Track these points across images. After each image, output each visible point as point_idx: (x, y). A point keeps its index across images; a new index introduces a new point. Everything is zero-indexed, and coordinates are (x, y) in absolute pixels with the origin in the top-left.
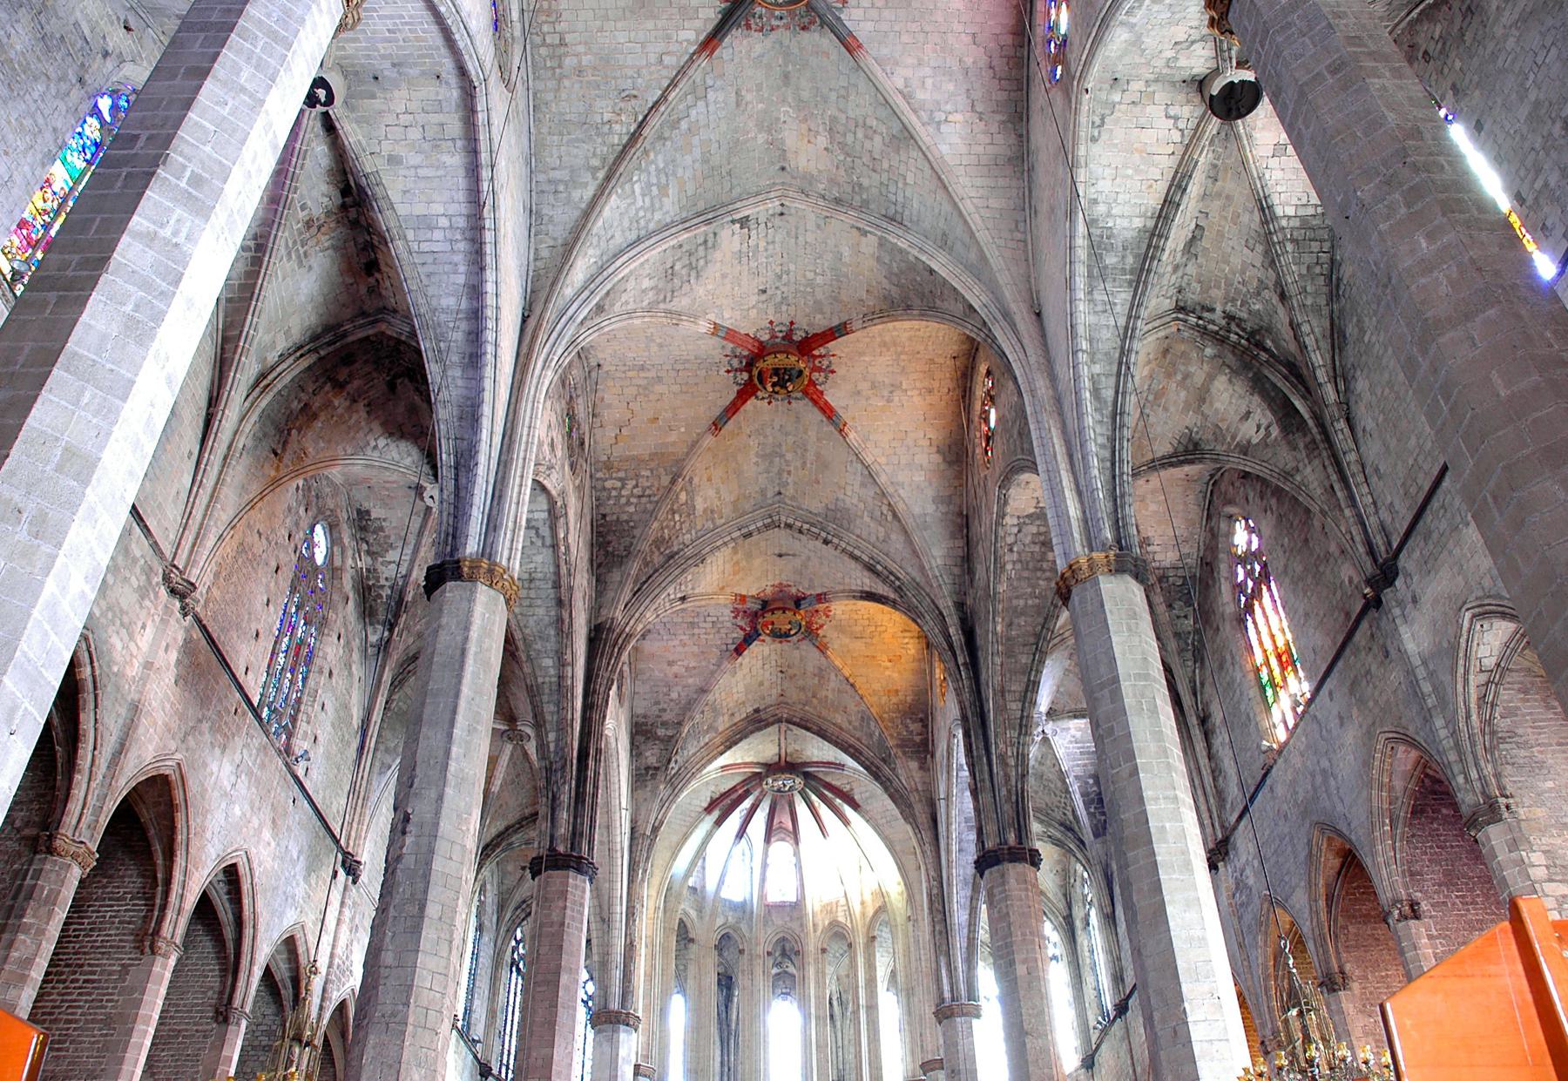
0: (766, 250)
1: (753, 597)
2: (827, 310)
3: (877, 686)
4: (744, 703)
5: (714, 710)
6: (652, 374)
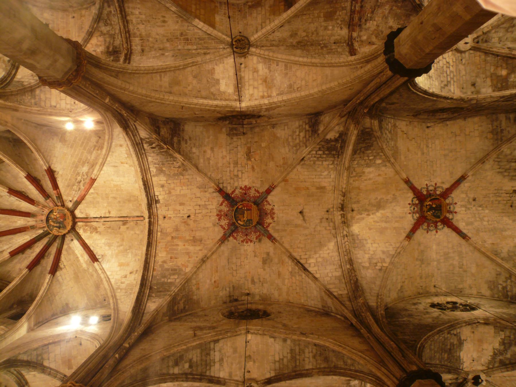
1: (266, 198)
2: (470, 227)
3: (201, 276)
4: (170, 193)
5: (175, 175)
6: (425, 151)
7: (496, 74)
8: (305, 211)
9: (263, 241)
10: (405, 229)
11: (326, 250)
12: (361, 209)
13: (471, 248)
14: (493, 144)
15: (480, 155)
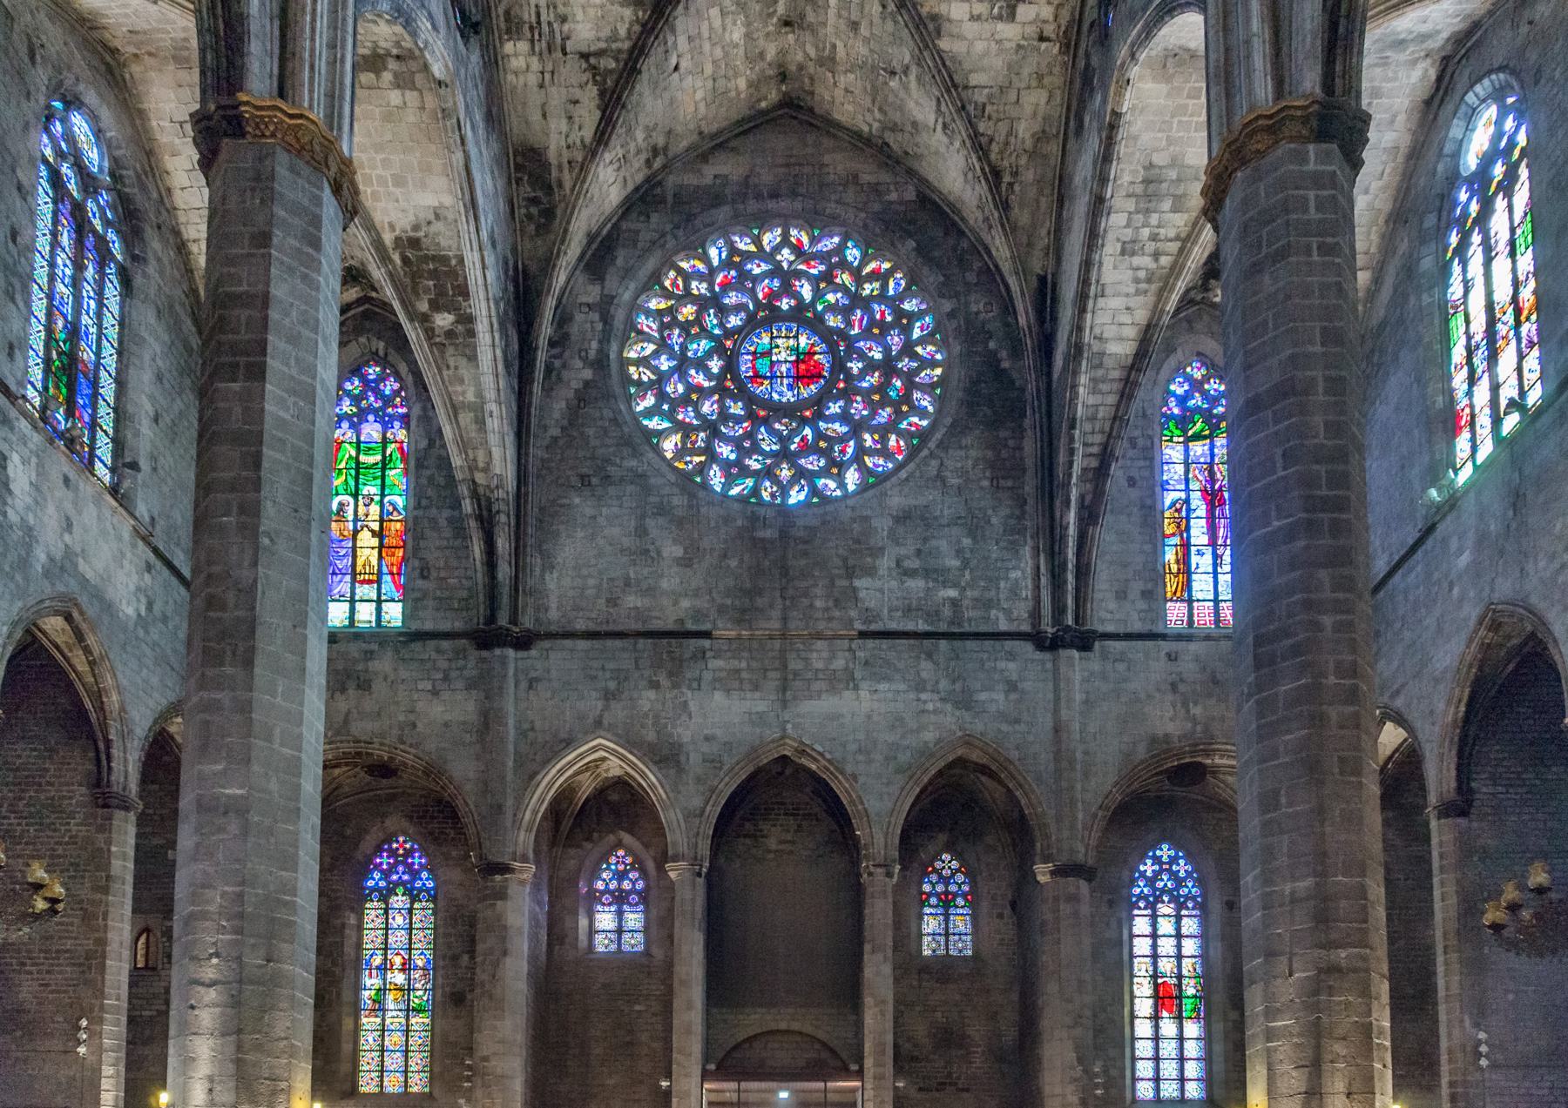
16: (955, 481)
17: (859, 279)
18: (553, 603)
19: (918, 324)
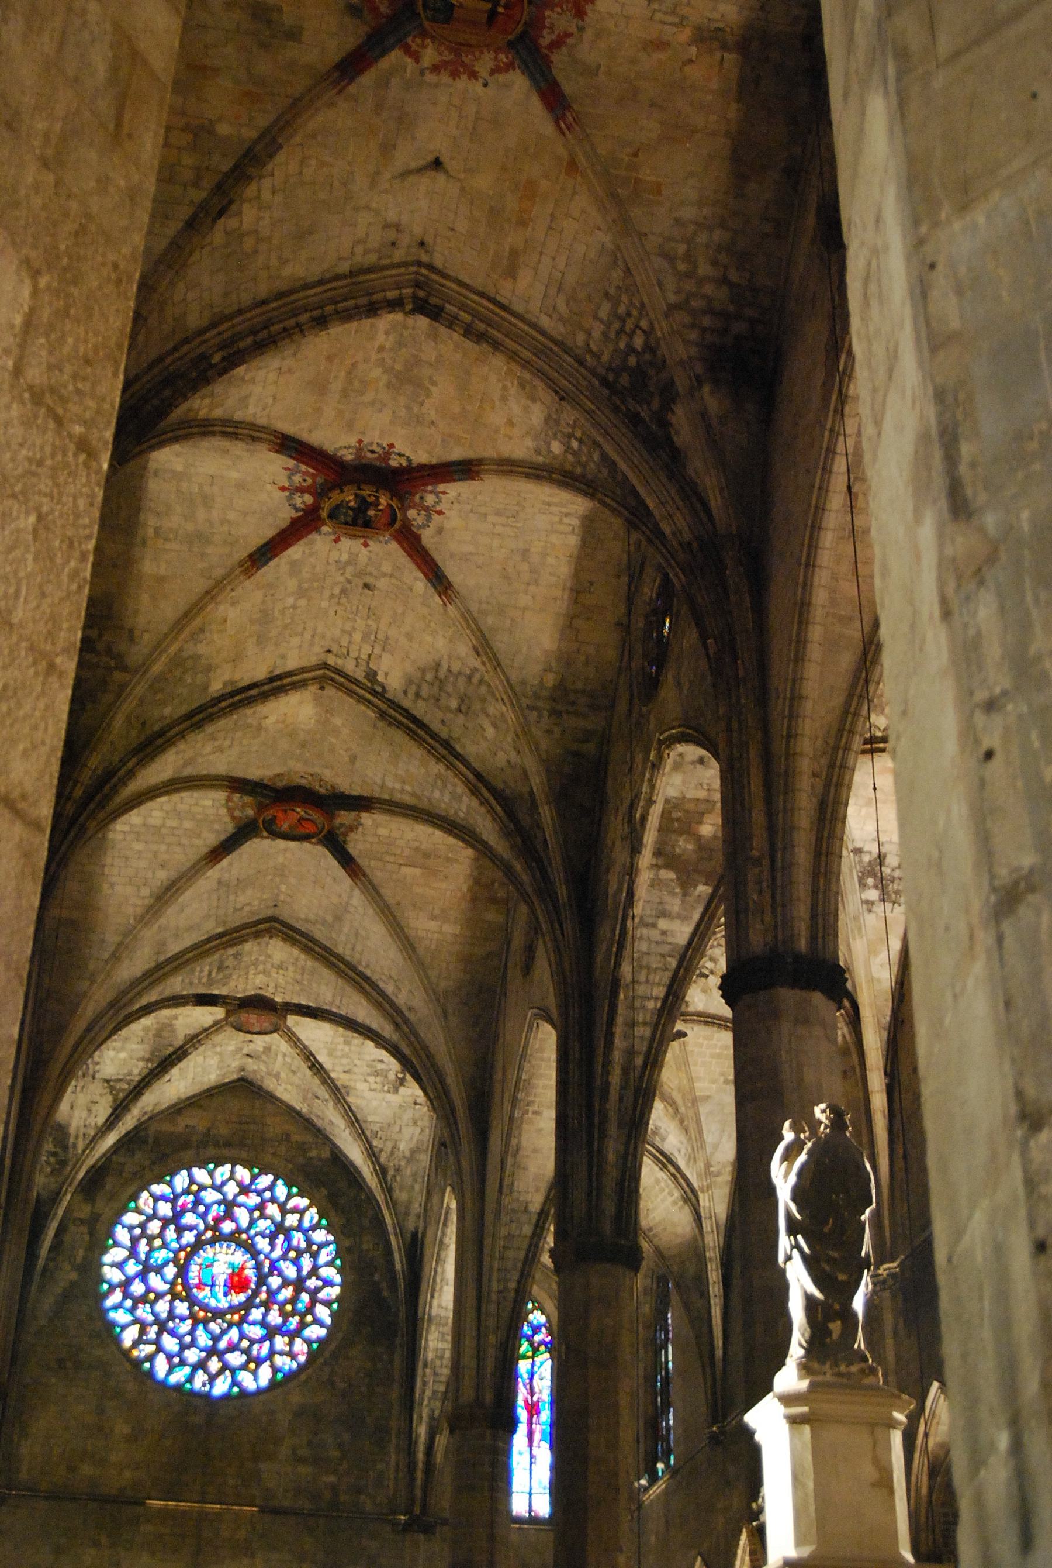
0: (354, 629)
7: (710, 813)
8: (441, 178)
9: (347, 19)
10: (310, 431)
11: (279, 258)
12: (405, 334)
13: (219, 572)
14: (524, 683)
15: (501, 643)
16: (341, 1385)
17: (284, 1212)
18: (24, 1467)
19: (324, 1252)
